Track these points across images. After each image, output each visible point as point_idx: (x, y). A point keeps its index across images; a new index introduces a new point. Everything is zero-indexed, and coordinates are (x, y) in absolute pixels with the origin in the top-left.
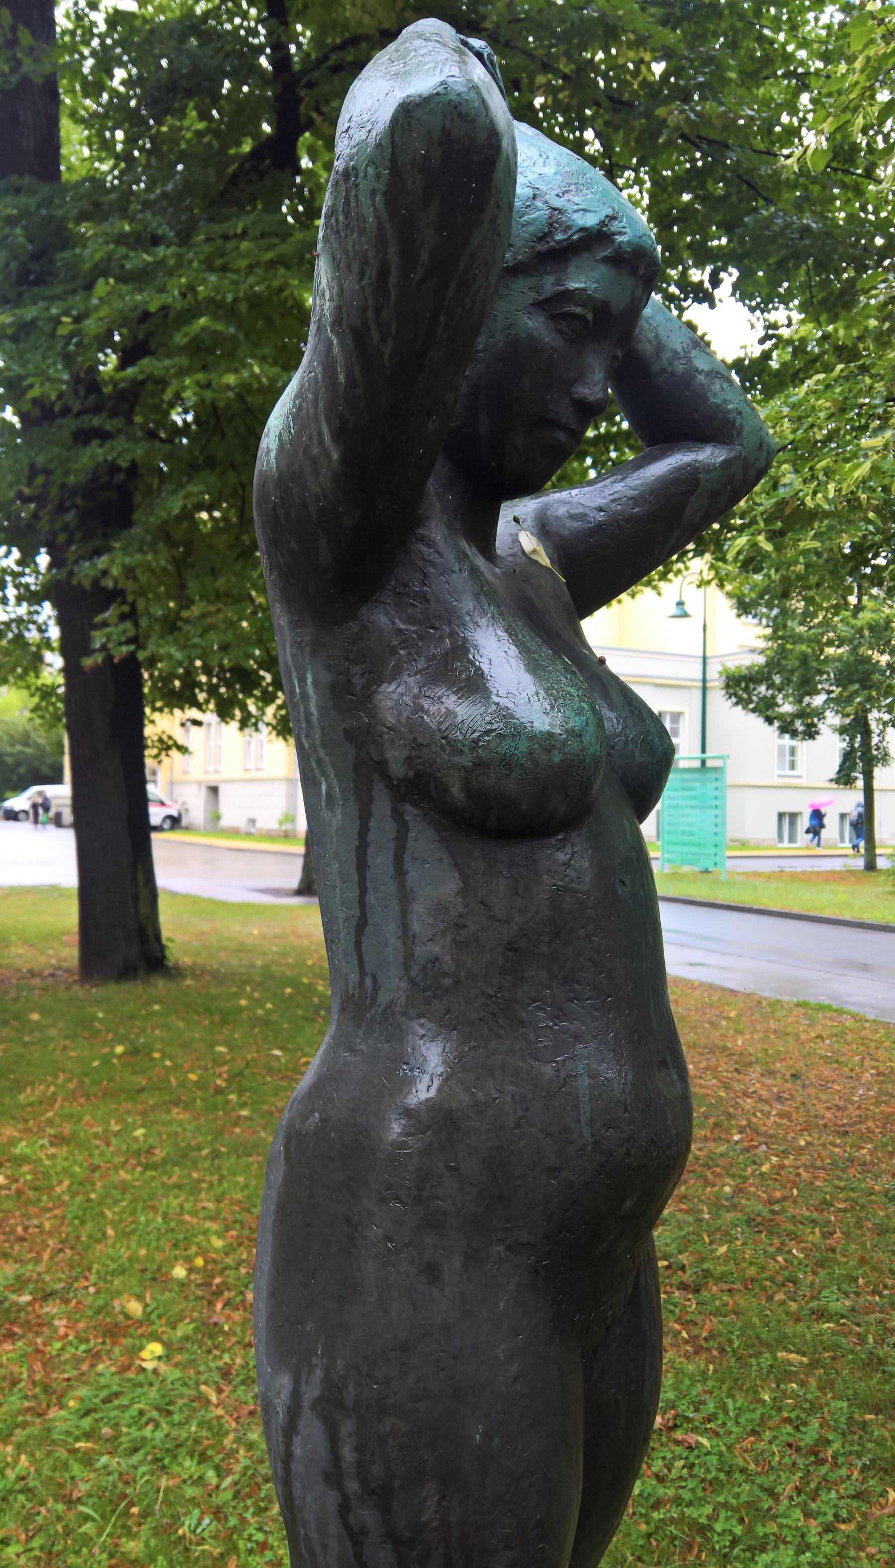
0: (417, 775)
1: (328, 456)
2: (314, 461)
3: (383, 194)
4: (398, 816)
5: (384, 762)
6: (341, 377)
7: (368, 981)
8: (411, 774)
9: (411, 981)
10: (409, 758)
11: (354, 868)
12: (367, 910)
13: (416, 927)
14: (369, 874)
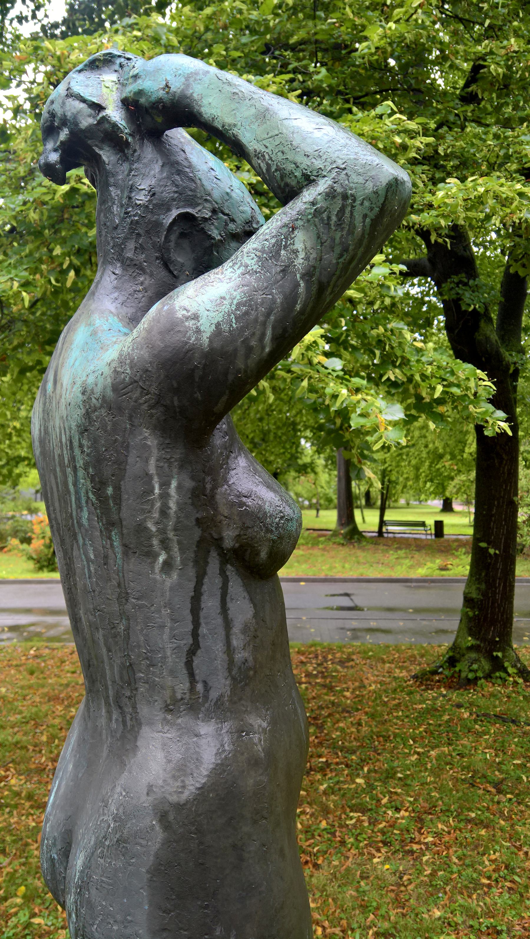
0: (241, 546)
1: (263, 348)
2: (249, 350)
3: (372, 220)
4: (223, 572)
5: (221, 539)
6: (298, 307)
7: (200, 687)
8: (237, 545)
9: (234, 679)
10: (239, 536)
11: (188, 611)
12: (200, 639)
13: (235, 643)
14: (202, 614)
